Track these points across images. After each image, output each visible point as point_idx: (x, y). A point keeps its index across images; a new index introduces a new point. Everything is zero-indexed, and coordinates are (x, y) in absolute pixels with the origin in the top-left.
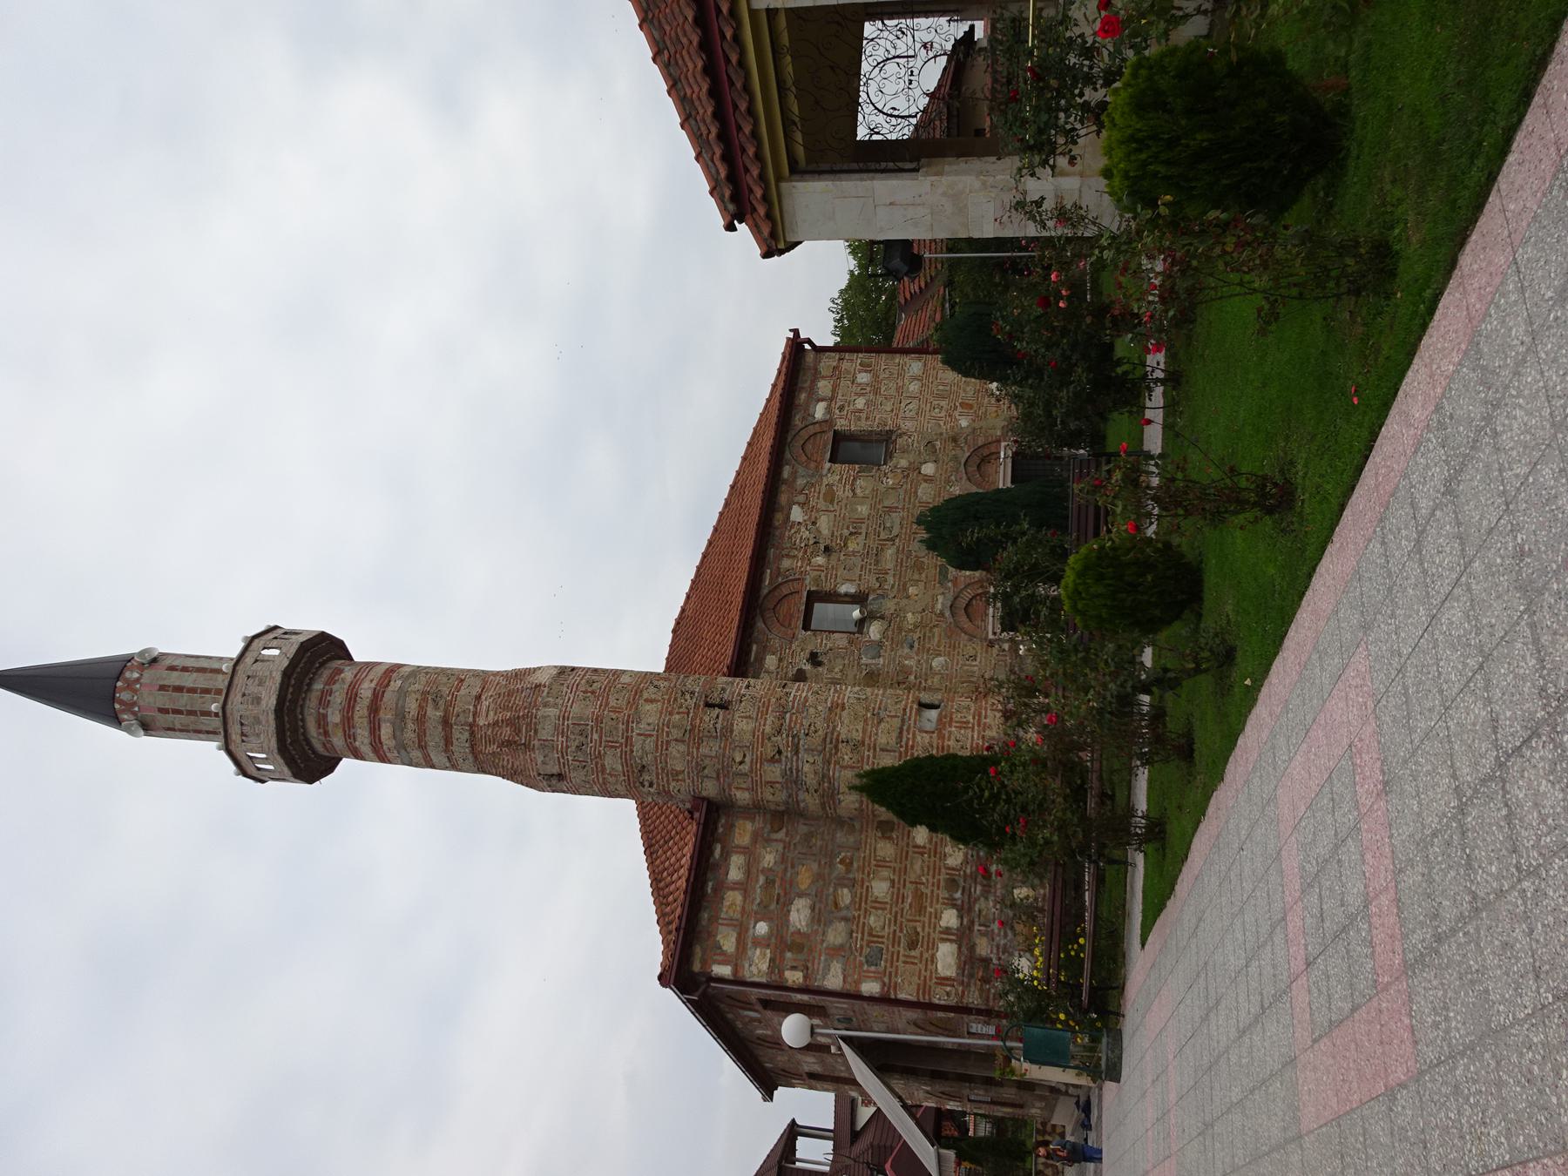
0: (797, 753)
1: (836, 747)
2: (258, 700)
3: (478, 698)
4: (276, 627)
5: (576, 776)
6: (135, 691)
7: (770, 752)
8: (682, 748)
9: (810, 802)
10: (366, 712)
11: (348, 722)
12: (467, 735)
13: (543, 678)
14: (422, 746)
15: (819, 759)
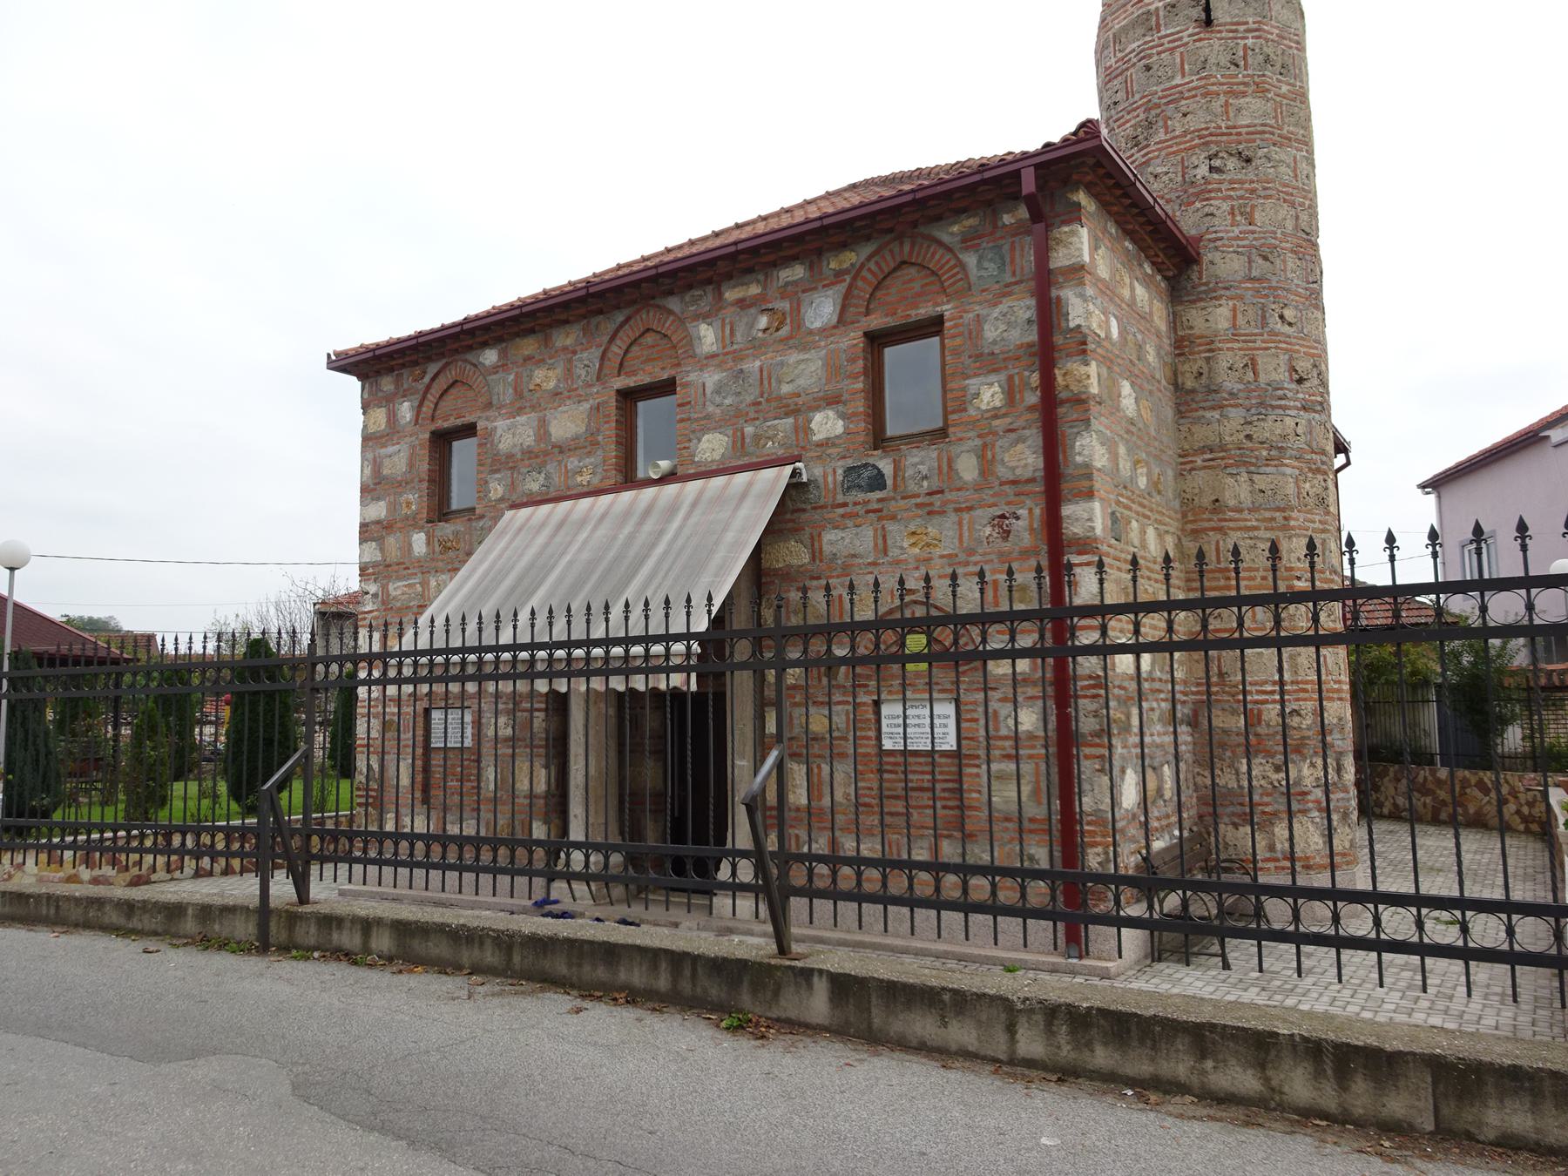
0: (1304, 408)
1: (1318, 471)
5: (1214, 48)
7: (1303, 365)
8: (1289, 224)
9: (1230, 425)
15: (1300, 443)
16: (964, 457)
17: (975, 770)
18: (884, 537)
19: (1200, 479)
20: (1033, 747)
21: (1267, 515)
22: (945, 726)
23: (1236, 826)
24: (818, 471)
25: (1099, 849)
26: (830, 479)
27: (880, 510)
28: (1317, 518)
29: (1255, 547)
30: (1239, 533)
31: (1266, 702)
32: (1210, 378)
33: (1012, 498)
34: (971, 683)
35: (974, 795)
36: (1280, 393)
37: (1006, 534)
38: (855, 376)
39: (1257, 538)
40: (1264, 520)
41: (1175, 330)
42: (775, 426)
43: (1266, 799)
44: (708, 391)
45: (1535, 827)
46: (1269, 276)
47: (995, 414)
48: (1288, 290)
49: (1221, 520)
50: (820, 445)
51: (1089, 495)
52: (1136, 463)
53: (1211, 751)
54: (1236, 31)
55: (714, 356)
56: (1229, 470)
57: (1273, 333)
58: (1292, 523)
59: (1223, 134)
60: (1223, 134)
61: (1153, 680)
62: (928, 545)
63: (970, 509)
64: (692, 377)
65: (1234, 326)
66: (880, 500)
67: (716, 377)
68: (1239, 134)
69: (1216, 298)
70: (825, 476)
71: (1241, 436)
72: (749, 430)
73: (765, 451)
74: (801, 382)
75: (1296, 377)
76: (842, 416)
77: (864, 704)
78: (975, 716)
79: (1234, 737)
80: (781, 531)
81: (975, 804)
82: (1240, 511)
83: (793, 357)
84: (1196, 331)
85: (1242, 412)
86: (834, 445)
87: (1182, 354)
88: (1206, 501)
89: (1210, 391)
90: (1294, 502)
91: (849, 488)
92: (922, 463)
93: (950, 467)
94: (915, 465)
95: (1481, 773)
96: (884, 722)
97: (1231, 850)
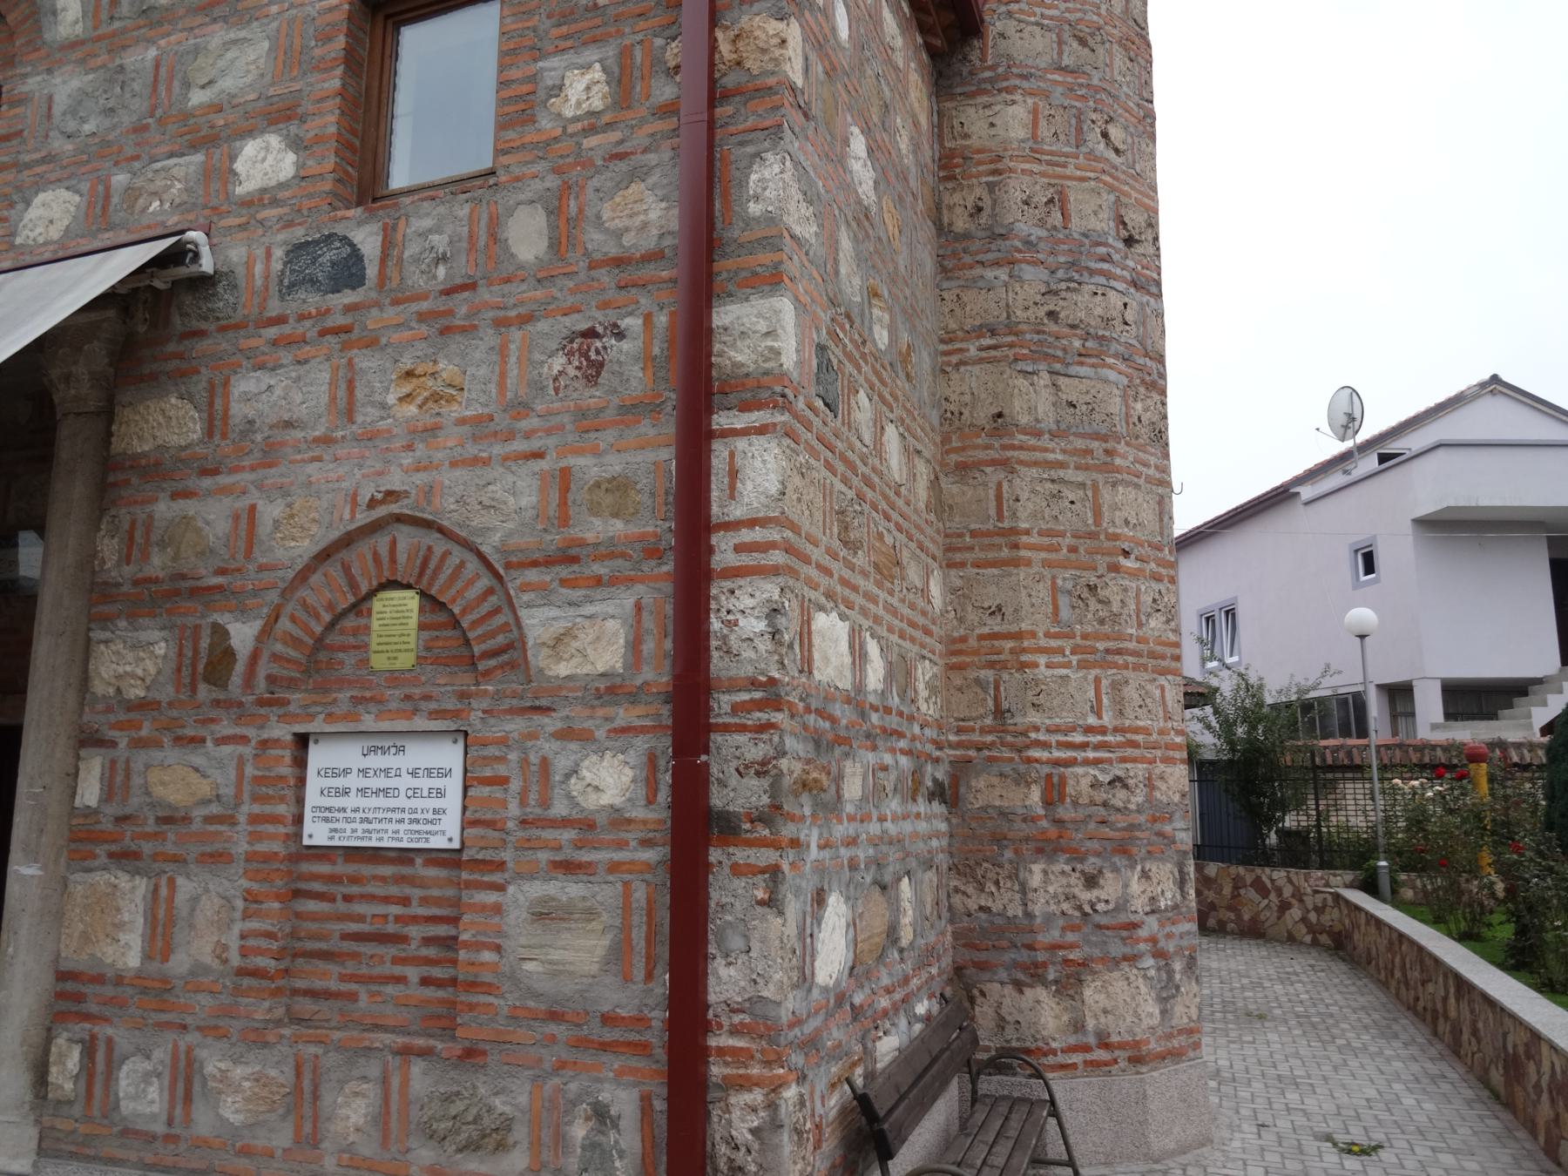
0: (1134, 284)
7: (1135, 218)
15: (1130, 336)
16: (522, 213)
17: (491, 897)
18: (351, 385)
19: (973, 379)
20: (621, 845)
21: (1080, 443)
22: (441, 793)
23: (1019, 986)
24: (236, 254)
25: (757, 1096)
26: (258, 269)
27: (347, 330)
28: (1153, 460)
29: (1058, 496)
30: (1034, 471)
31: (1071, 763)
32: (993, 216)
33: (612, 294)
34: (498, 696)
35: (487, 956)
36: (1102, 250)
37: (594, 370)
38: (322, 67)
39: (1062, 481)
40: (1075, 452)
41: (940, 137)
42: (166, 169)
43: (1071, 937)
44: (57, 110)
45: (1324, 939)
46: (1088, 69)
47: (592, 124)
49: (1004, 447)
50: (248, 203)
51: (773, 280)
52: (874, 294)
53: (981, 847)
55: (74, 44)
56: (1021, 366)
57: (1091, 156)
58: (1118, 461)
61: (888, 710)
62: (436, 397)
63: (526, 319)
64: (32, 84)
65: (1034, 137)
66: (349, 309)
67: (75, 83)
69: (1008, 90)
70: (249, 265)
71: (1042, 312)
72: (120, 179)
73: (145, 221)
74: (228, 84)
75: (1124, 234)
76: (296, 144)
77: (276, 743)
78: (502, 770)
79: (1018, 825)
80: (154, 377)
81: (487, 977)
82: (1038, 434)
83: (218, 35)
84: (974, 142)
85: (1043, 274)
86: (275, 202)
87: (953, 178)
88: (983, 415)
89: (994, 237)
90: (1121, 428)
91: (292, 285)
92: (437, 230)
93: (494, 237)
94: (424, 235)
95: (1258, 871)
96: (314, 783)
97: (1010, 1032)
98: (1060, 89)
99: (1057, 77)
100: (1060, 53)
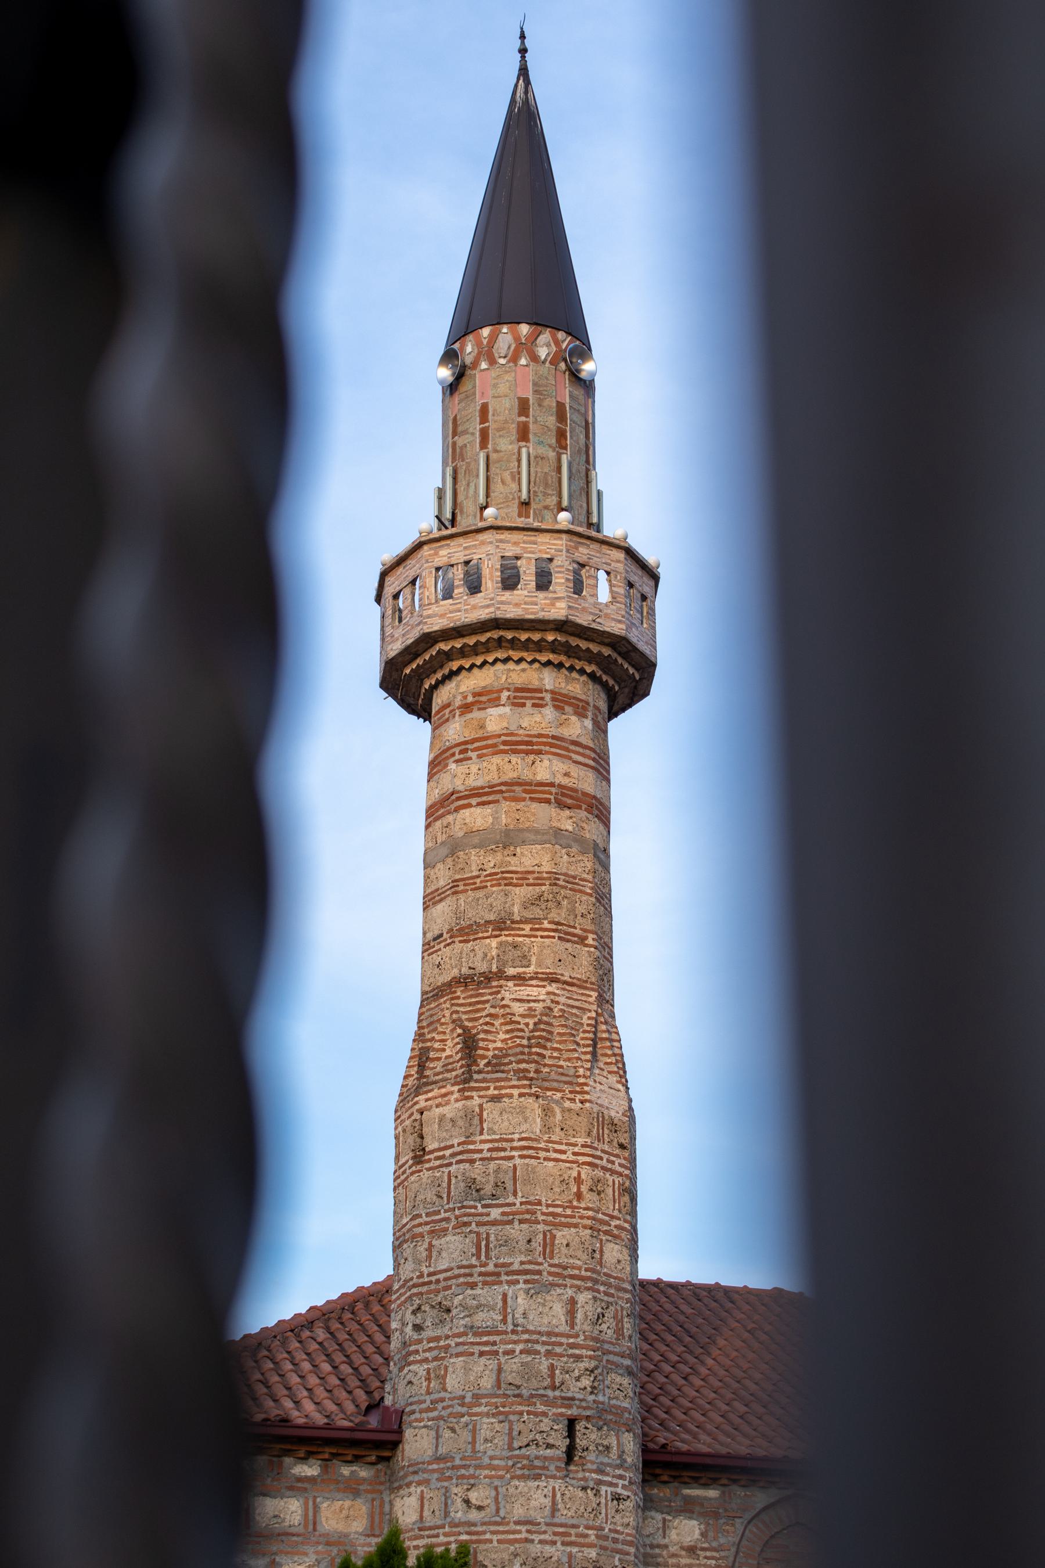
2: (510, 581)
3: (553, 979)
4: (655, 578)
6: (515, 359)
8: (487, 1383)
10: (510, 775)
11: (484, 745)
12: (482, 967)
13: (601, 1092)
14: (455, 888)
48: (477, 1467)
54: (443, 1157)
59: (424, 1284)
60: (424, 1284)
65: (421, 1517)
68: (438, 1281)
69: (408, 1485)
98: (436, 1476)
99: (435, 1466)
100: (437, 1447)
